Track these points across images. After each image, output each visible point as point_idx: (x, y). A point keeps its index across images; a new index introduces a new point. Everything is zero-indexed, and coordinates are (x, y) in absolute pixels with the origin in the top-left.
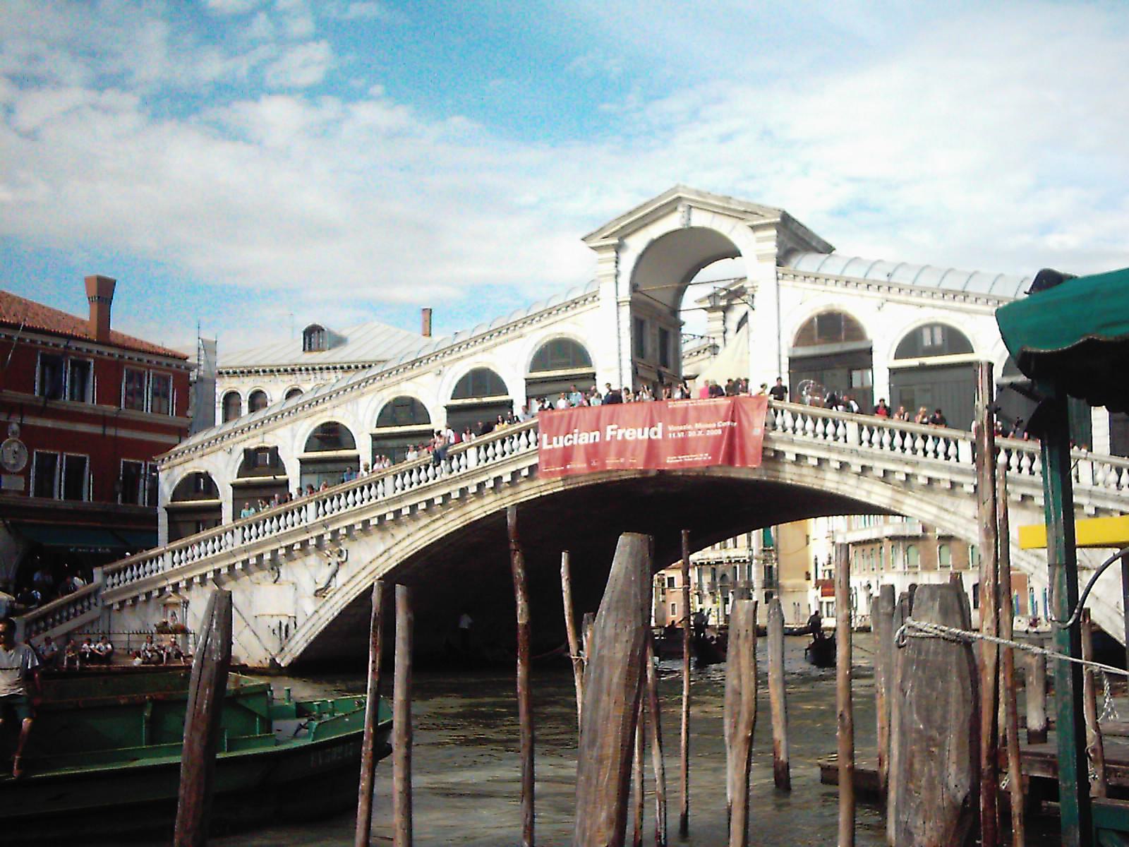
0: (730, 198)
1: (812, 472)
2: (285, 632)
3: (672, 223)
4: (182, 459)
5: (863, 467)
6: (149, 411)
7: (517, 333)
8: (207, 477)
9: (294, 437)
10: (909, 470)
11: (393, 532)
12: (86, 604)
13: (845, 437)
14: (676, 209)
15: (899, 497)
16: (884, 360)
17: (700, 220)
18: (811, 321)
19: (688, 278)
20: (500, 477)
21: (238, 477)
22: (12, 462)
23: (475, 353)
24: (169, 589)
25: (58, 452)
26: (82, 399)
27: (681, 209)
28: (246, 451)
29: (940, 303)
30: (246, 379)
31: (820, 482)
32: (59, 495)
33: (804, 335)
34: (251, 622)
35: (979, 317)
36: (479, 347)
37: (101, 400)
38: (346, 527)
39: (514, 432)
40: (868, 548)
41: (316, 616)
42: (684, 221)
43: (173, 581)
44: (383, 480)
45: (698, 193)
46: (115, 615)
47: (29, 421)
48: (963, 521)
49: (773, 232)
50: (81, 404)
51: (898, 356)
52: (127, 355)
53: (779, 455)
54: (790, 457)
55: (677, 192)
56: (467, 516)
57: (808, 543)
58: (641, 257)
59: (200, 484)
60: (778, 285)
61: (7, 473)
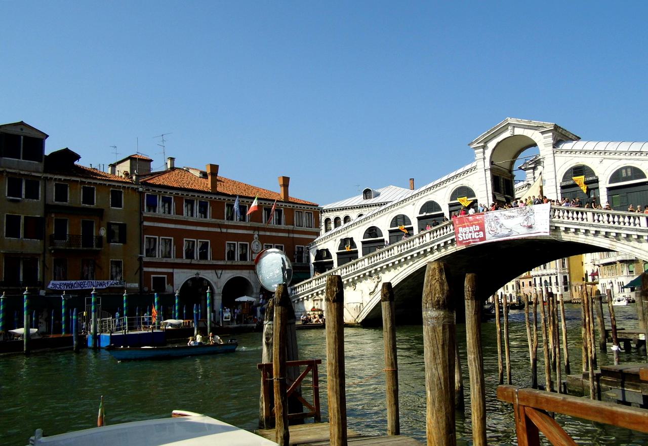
1: (574, 235)
2: (360, 309)
5: (596, 232)
7: (445, 185)
8: (327, 250)
9: (359, 233)
10: (617, 231)
13: (587, 219)
14: (507, 129)
15: (613, 243)
16: (604, 185)
17: (518, 131)
18: (571, 169)
19: (516, 156)
21: (339, 250)
22: (256, 249)
23: (427, 195)
24: (315, 294)
27: (510, 128)
28: (341, 240)
29: (630, 157)
30: (342, 212)
31: (577, 239)
33: (565, 177)
36: (429, 192)
39: (444, 226)
40: (610, 266)
41: (371, 303)
42: (511, 133)
46: (296, 305)
47: (262, 233)
49: (551, 134)
50: (279, 226)
51: (611, 182)
52: (296, 206)
53: (556, 227)
57: (583, 265)
58: (494, 150)
60: (554, 157)
61: (254, 253)
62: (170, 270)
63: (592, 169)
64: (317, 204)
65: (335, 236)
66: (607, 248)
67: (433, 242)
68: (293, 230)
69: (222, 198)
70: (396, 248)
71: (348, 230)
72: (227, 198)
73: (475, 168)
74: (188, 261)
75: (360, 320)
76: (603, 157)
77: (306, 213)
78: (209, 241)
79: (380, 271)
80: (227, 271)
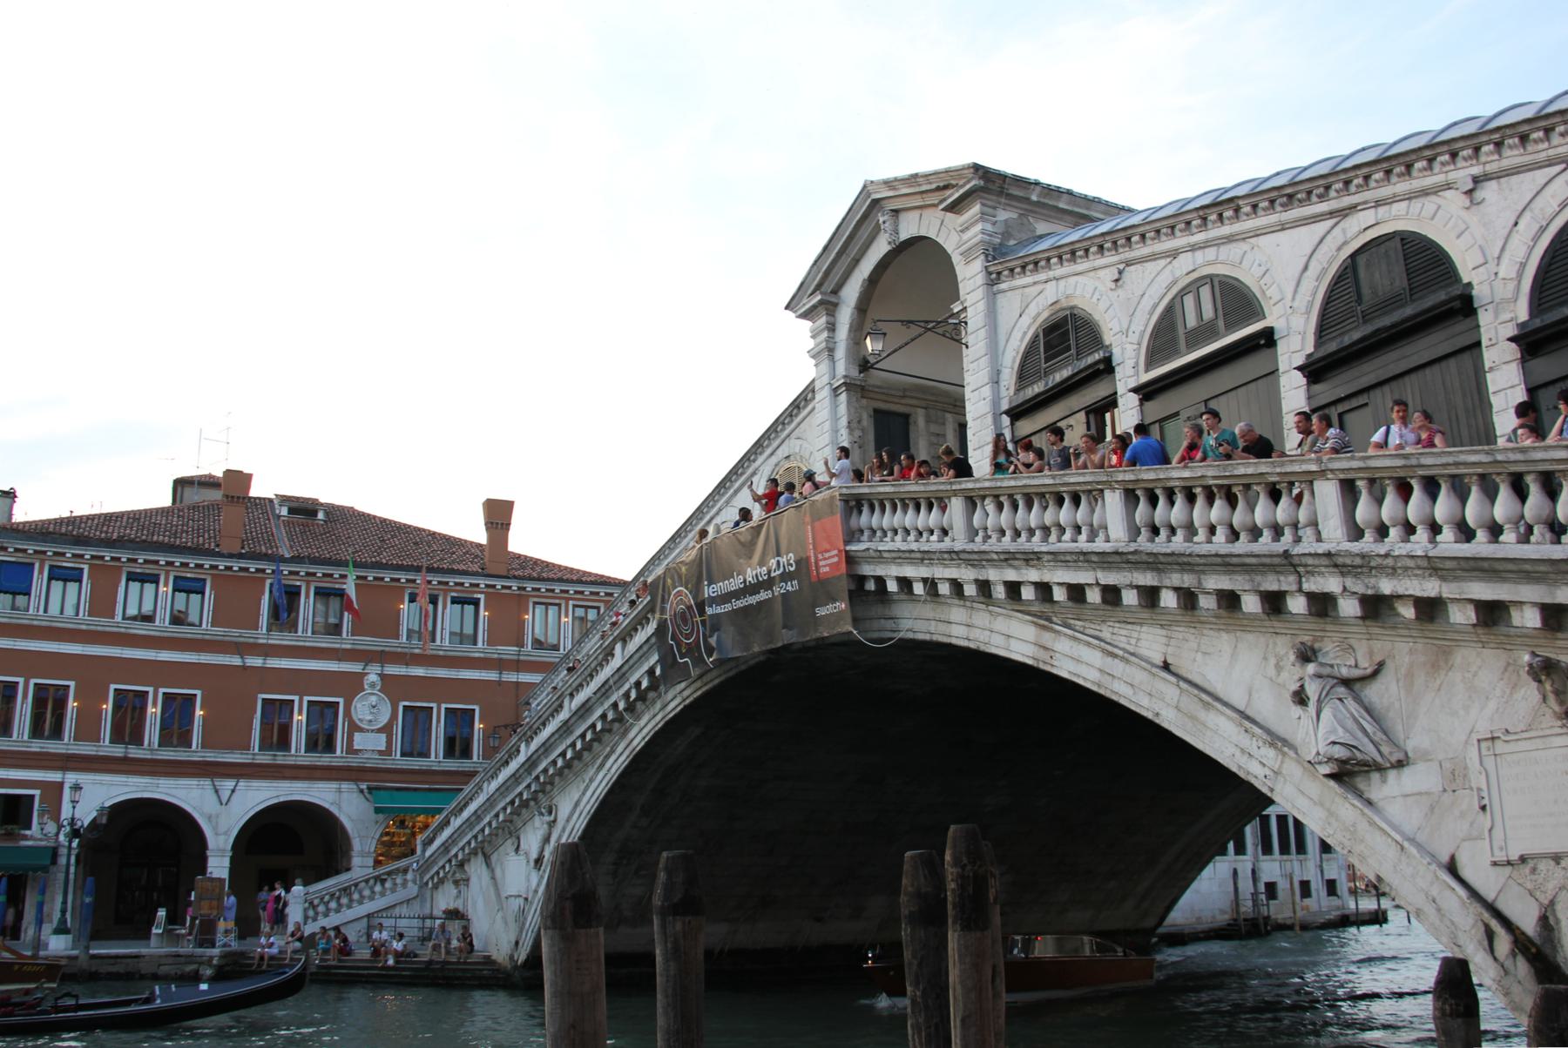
0: (916, 176)
3: (880, 248)
10: (1033, 575)
15: (1047, 638)
17: (910, 227)
20: (638, 684)
25: (434, 705)
26: (475, 643)
29: (1200, 237)
32: (437, 758)
35: (1263, 241)
45: (888, 183)
47: (393, 670)
48: (1139, 676)
51: (1151, 363)
52: (529, 586)
53: (880, 581)
54: (892, 586)
55: (869, 195)
58: (862, 308)
61: (361, 730)
62: (55, 776)
63: (1096, 317)
66: (1030, 662)
67: (621, 674)
68: (518, 661)
69: (253, 566)
73: (810, 390)
74: (118, 751)
76: (1122, 257)
77: (575, 606)
78: (198, 693)
80: (256, 783)
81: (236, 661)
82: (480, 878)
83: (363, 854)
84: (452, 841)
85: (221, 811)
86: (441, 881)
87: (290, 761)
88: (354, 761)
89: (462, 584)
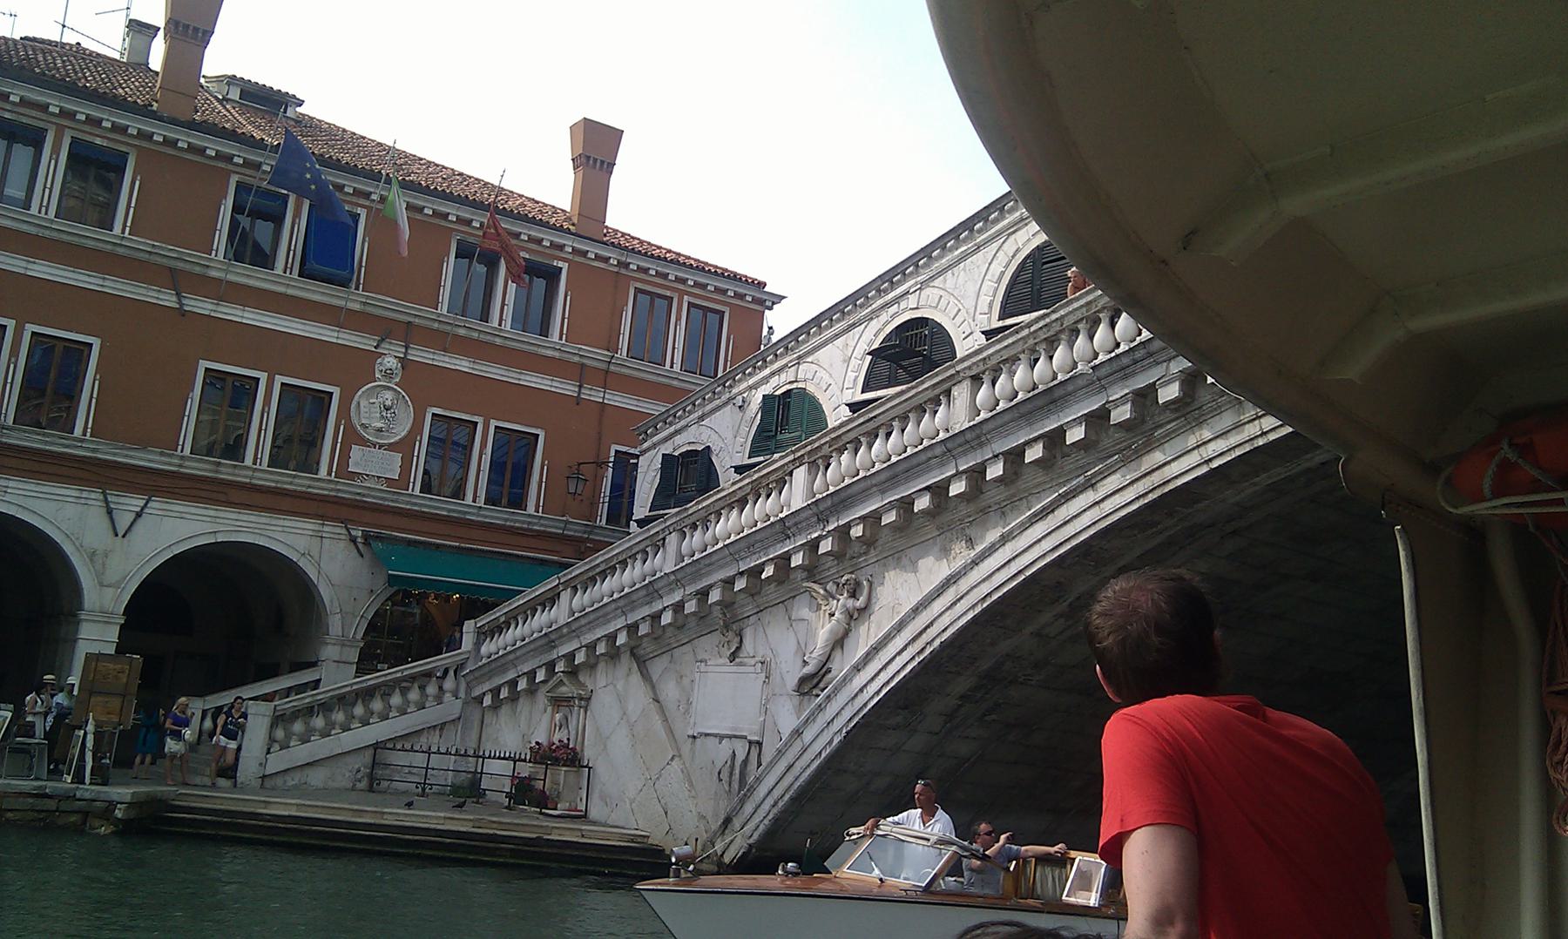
2: (738, 780)
4: (672, 429)
6: (677, 368)
11: (971, 532)
12: (431, 689)
22: (379, 425)
26: (544, 331)
34: (686, 747)
37: (571, 336)
38: (863, 519)
43: (564, 650)
44: (948, 393)
47: (419, 355)
56: (1156, 478)
59: (690, 475)
61: (364, 442)
64: (761, 278)
65: (744, 385)
69: (213, 146)
70: (961, 393)
71: (804, 349)
72: (240, 155)
75: (735, 846)
78: (96, 342)
79: (868, 542)
80: (179, 507)
81: (168, 299)
82: (621, 699)
83: (343, 643)
84: (572, 629)
85: (114, 548)
86: (514, 697)
87: (242, 478)
88: (346, 490)
89: (539, 242)
